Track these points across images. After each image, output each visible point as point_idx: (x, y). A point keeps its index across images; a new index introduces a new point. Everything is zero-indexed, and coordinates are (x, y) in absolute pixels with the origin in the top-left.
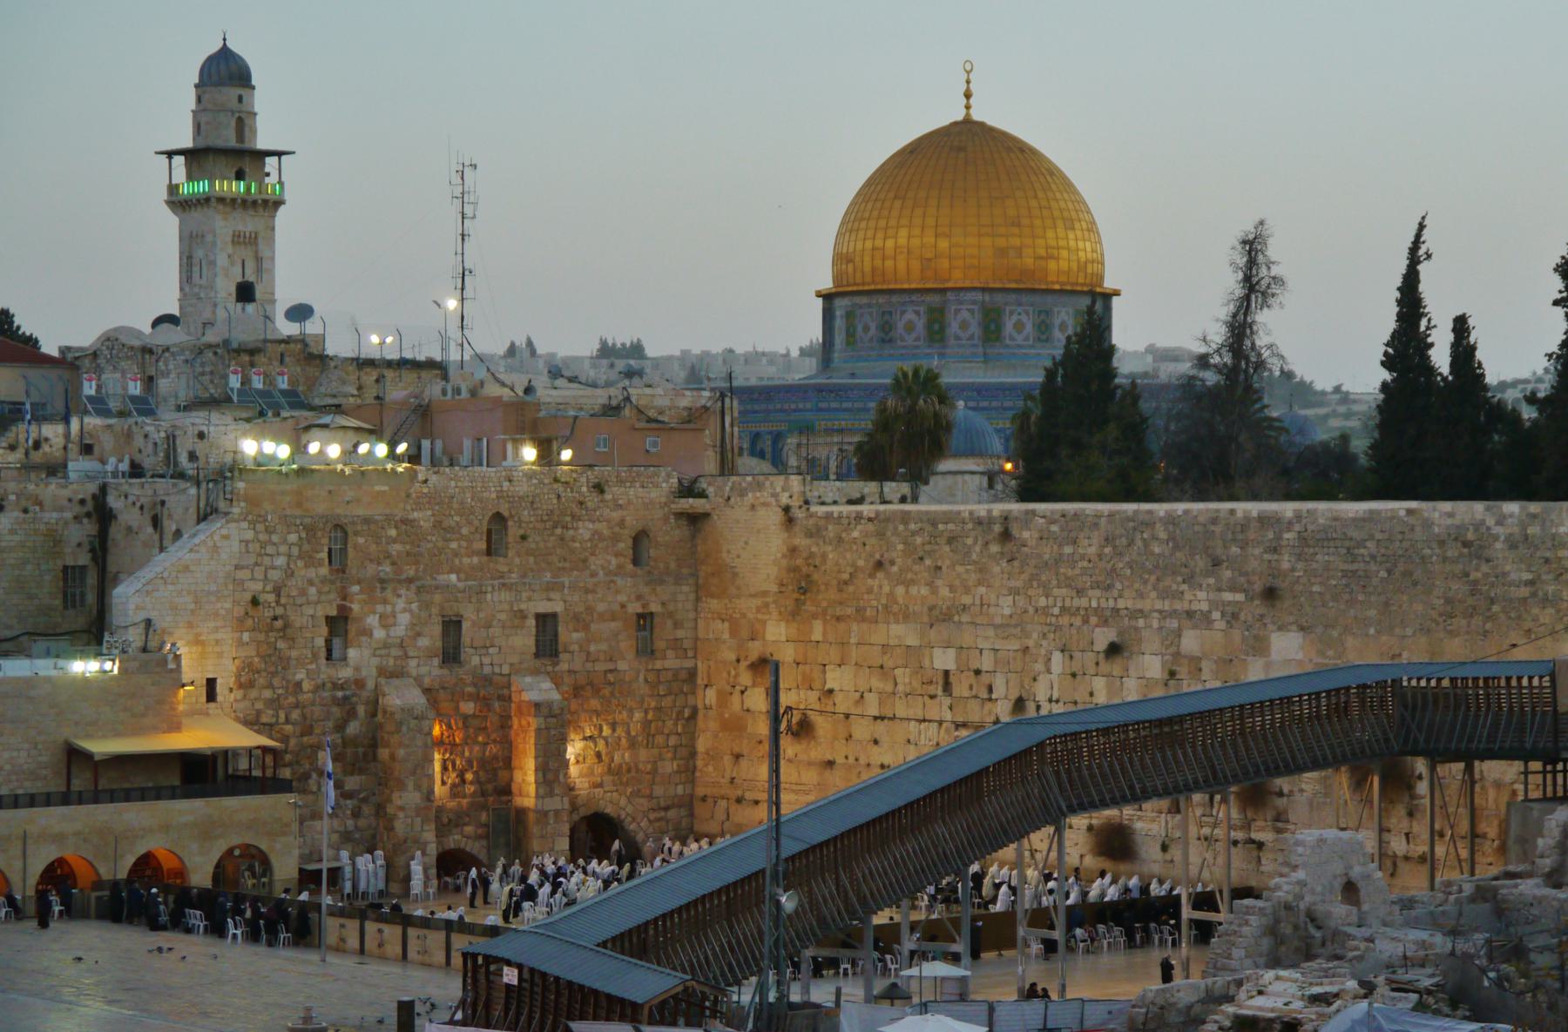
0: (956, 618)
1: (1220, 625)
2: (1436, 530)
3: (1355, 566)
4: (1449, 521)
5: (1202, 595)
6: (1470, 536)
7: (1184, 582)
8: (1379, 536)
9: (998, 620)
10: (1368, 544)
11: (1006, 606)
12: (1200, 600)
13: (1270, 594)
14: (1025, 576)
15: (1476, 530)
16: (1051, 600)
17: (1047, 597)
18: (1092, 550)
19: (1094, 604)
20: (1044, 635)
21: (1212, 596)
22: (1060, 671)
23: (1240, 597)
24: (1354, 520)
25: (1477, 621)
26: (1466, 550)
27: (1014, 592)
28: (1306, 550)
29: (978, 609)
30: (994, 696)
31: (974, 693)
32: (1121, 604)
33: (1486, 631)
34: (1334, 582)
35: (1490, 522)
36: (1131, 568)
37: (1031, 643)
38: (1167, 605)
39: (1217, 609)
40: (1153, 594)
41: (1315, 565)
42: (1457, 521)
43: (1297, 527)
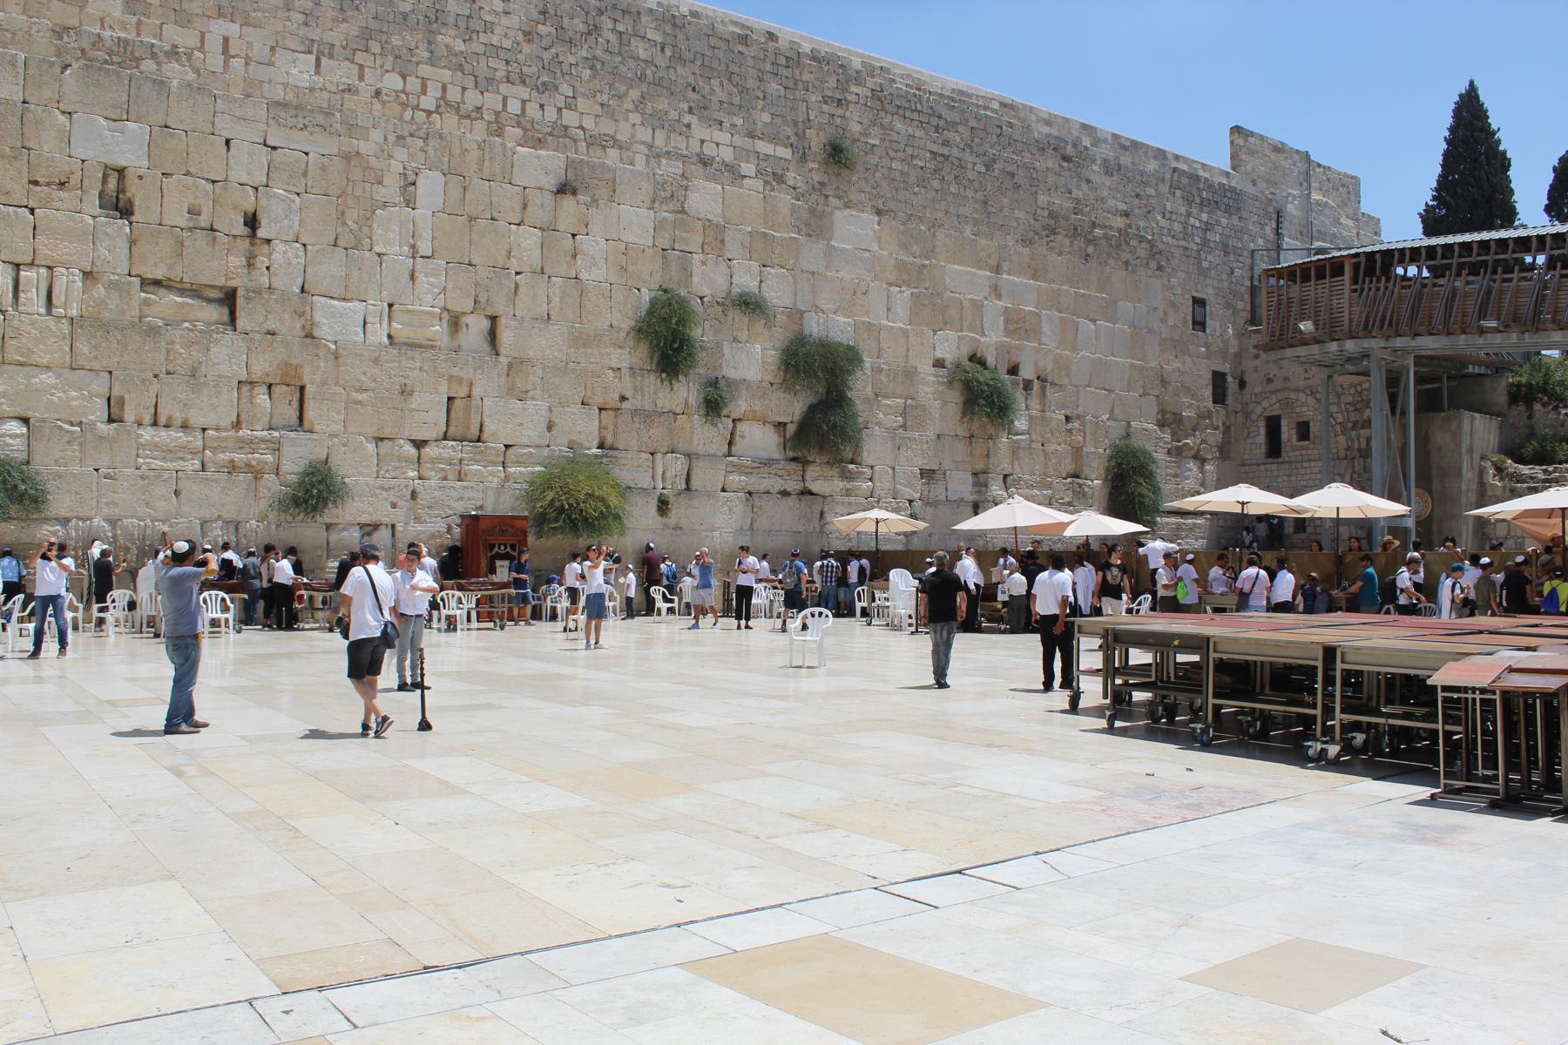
0: (148, 65)
1: (758, 184)
2: (1036, 135)
3: (946, 151)
4: (1046, 130)
5: (723, 137)
6: (1069, 151)
7: (691, 111)
8: (973, 123)
9: (279, 93)
10: (961, 129)
11: (298, 71)
12: (721, 143)
13: (837, 154)
14: (350, 29)
15: (1075, 146)
16: (413, 84)
17: (404, 77)
18: (513, 21)
19: (514, 107)
20: (401, 138)
21: (739, 141)
22: (440, 207)
23: (786, 153)
24: (942, 96)
25: (1079, 243)
26: (1065, 164)
27: (321, 53)
28: (882, 114)
29: (215, 61)
30: (261, 233)
31: (204, 221)
32: (570, 118)
33: (1088, 255)
34: (920, 164)
35: (1087, 142)
36: (592, 68)
37: (367, 147)
38: (660, 137)
39: (748, 162)
40: (635, 118)
41: (894, 137)
42: (1054, 132)
43: (870, 82)
